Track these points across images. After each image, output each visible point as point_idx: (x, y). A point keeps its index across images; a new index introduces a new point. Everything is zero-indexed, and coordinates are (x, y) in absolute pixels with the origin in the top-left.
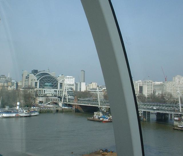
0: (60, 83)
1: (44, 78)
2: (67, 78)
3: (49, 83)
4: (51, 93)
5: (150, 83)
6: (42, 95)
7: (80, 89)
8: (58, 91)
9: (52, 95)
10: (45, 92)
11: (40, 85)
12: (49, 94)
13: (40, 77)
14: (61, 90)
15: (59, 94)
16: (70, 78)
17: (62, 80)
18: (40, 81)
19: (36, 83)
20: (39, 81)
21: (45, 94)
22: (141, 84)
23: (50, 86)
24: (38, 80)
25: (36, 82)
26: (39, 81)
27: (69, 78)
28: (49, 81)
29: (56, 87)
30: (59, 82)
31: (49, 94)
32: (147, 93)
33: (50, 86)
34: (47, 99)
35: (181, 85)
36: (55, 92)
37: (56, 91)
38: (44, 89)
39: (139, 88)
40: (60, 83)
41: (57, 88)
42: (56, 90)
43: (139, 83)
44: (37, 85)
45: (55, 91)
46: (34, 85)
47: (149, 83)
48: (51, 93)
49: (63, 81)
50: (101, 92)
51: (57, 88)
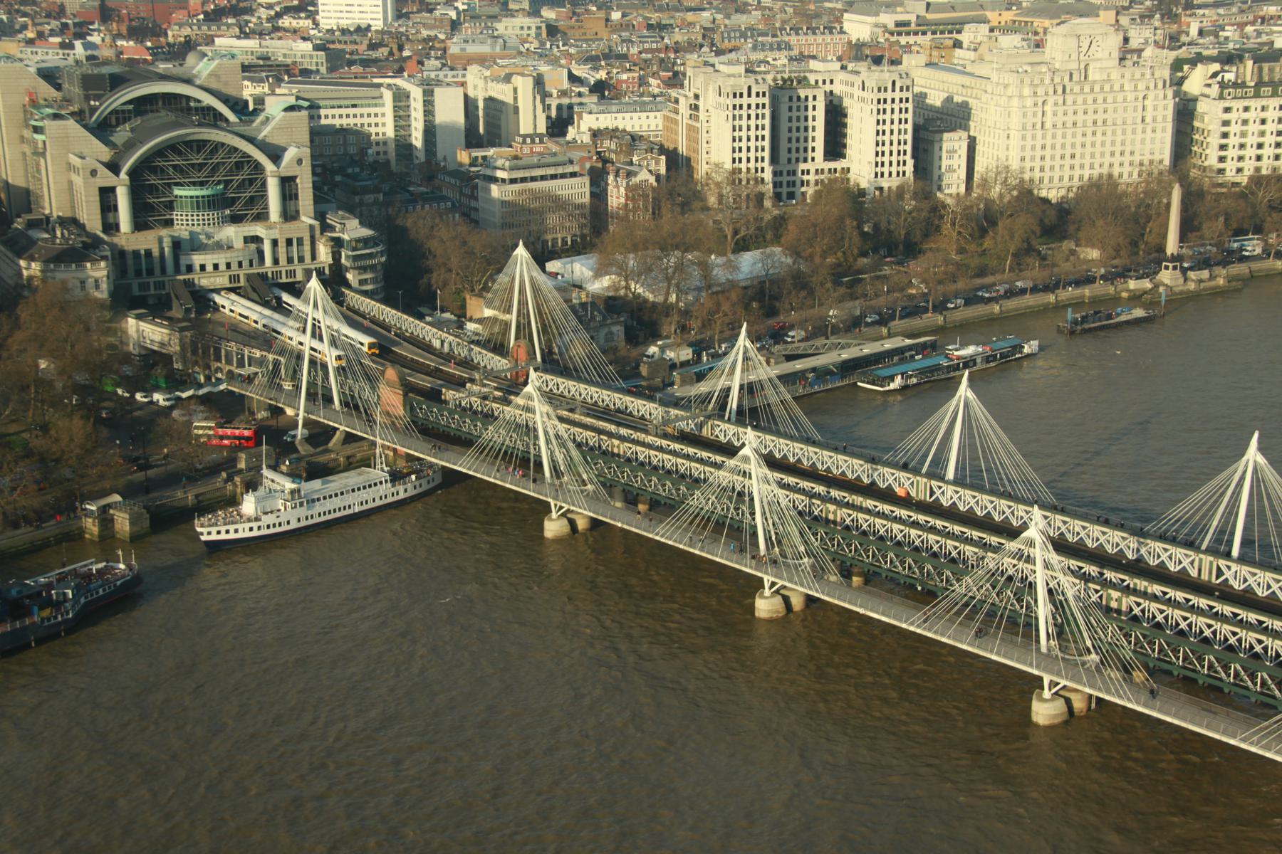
1: (159, 152)
3: (202, 184)
4: (222, 267)
6: (160, 285)
8: (275, 243)
9: (234, 279)
10: (184, 261)
12: (209, 268)
13: (130, 146)
14: (294, 230)
15: (283, 266)
18: (132, 173)
19: (107, 195)
20: (123, 175)
26: (123, 175)
28: (201, 166)
29: (253, 209)
31: (209, 268)
35: (1097, 89)
37: (257, 240)
41: (262, 217)
44: (116, 208)
46: (91, 218)
48: (222, 267)
49: (300, 162)
50: (573, 175)
51: (262, 217)
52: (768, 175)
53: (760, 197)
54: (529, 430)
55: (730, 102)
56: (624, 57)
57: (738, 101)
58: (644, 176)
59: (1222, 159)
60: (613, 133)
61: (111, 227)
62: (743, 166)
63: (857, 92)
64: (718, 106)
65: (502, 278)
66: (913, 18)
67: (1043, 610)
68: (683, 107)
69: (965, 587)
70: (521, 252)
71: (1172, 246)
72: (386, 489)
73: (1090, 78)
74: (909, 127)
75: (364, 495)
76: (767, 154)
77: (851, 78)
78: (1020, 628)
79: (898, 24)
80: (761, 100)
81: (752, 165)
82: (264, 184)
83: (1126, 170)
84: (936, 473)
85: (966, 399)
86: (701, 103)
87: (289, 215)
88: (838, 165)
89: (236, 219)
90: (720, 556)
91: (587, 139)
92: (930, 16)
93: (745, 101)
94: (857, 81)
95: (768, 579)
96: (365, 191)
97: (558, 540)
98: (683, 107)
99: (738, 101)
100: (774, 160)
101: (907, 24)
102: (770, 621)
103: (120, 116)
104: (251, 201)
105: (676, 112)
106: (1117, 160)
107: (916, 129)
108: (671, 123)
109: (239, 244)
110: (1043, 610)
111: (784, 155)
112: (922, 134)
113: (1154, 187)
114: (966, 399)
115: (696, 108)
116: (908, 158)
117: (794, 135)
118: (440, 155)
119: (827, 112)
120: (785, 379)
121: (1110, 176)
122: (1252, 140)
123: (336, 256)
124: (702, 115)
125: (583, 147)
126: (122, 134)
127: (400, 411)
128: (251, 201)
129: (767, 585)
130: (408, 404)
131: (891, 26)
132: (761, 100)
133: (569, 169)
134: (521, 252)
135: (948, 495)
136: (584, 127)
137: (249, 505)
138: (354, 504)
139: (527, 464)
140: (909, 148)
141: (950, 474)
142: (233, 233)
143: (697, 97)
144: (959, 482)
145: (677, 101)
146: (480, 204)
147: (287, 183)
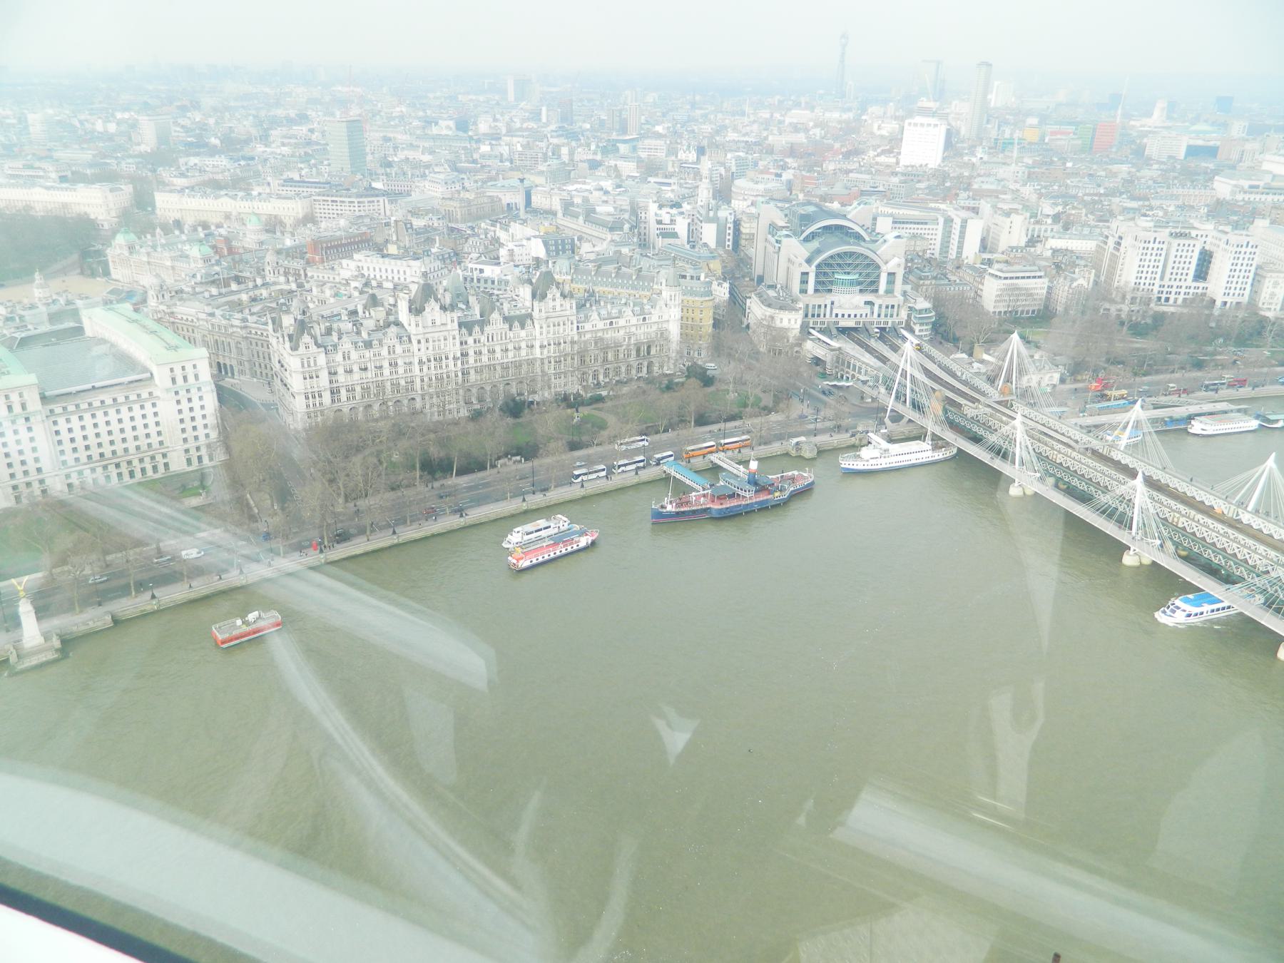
0: (889, 274)
2: (916, 125)
6: (823, 323)
7: (960, 247)
8: (880, 306)
10: (835, 312)
11: (818, 282)
13: (818, 252)
14: (890, 301)
16: (929, 125)
17: (895, 261)
18: (818, 266)
21: (834, 319)
22: (1209, 240)
23: (852, 283)
24: (809, 261)
25: (803, 274)
26: (813, 267)
27: (922, 125)
30: (884, 268)
32: (1224, 285)
33: (852, 283)
34: (838, 358)
36: (868, 310)
37: (870, 303)
38: (827, 299)
39: (1195, 261)
40: (889, 274)
42: (870, 297)
45: (867, 303)
51: (877, 291)
52: (1156, 289)
54: (1012, 441)
55: (1143, 245)
56: (1075, 197)
58: (1081, 281)
60: (1066, 252)
61: (804, 291)
63: (1223, 245)
65: (1004, 346)
66: (1261, 184)
68: (1111, 242)
70: (1015, 337)
72: (930, 453)
75: (919, 455)
76: (1158, 276)
77: (1220, 235)
79: (1251, 187)
82: (879, 276)
84: (1242, 504)
85: (1271, 470)
86: (1123, 242)
87: (889, 292)
88: (1201, 285)
89: (861, 291)
90: (1109, 528)
91: (1049, 253)
92: (1275, 184)
93: (1151, 245)
94: (1224, 238)
96: (926, 278)
97: (1016, 498)
98: (1111, 242)
100: (1162, 278)
101: (1257, 187)
102: (1130, 567)
103: (813, 236)
104: (873, 283)
105: (1106, 243)
107: (1258, 267)
108: (1100, 250)
109: (862, 304)
111: (1167, 276)
112: (1260, 271)
114: (1271, 470)
115: (1119, 244)
116: (1248, 287)
117: (1176, 265)
118: (964, 256)
119: (1201, 253)
120: (1154, 421)
123: (909, 316)
124: (1122, 249)
125: (1046, 259)
126: (815, 244)
127: (941, 413)
128: (873, 283)
130: (945, 411)
131: (1246, 187)
133: (1038, 274)
134: (1015, 337)
135: (1246, 518)
136: (1048, 246)
137: (865, 452)
138: (913, 459)
139: (1002, 454)
140: (1250, 281)
142: (860, 299)
143: (1121, 238)
144: (1257, 512)
145: (1107, 237)
146: (984, 288)
147: (891, 275)
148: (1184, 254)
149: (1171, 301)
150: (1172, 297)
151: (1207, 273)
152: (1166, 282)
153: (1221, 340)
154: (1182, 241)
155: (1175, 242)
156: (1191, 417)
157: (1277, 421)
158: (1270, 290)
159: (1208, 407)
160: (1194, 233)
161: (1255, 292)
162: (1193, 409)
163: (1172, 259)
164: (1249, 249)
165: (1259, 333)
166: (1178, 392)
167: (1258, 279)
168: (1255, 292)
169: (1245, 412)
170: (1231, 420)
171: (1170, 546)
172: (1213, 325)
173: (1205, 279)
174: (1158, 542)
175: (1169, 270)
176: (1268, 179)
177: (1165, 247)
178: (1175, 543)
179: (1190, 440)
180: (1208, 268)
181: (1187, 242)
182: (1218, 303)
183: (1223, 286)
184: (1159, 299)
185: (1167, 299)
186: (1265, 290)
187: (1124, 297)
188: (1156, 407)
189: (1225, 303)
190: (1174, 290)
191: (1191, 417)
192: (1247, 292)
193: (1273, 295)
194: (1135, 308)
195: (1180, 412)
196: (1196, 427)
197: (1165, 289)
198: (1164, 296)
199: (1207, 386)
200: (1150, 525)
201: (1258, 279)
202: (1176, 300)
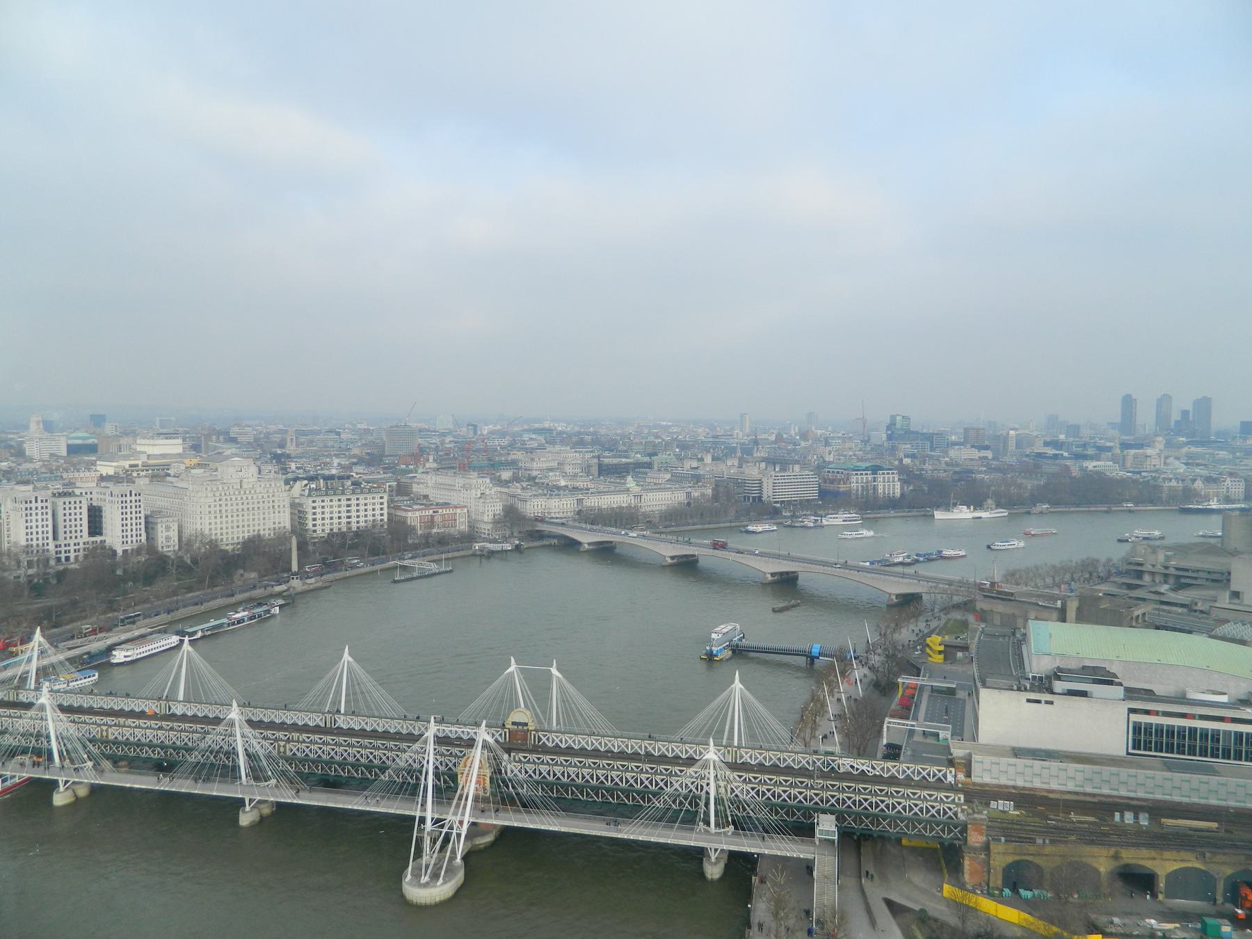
5: (133, 498)
22: (94, 496)
32: (120, 534)
43: (89, 496)
47: (128, 498)
52: (51, 547)
53: (48, 560)
55: (24, 506)
57: (28, 505)
59: (314, 525)
62: (34, 543)
63: (108, 498)
64: (15, 509)
66: (139, 463)
67: (242, 761)
69: (192, 758)
71: (295, 567)
73: (245, 486)
74: (142, 515)
76: (50, 535)
78: (230, 773)
79: (131, 466)
80: (44, 504)
81: (40, 542)
83: (267, 532)
88: (98, 539)
92: (151, 462)
95: (61, 780)
99: (28, 505)
100: (55, 538)
101: (137, 466)
106: (262, 527)
107: (146, 517)
110: (242, 761)
111: (61, 535)
112: (151, 520)
113: (281, 538)
117: (68, 523)
121: (259, 535)
122: (327, 516)
129: (61, 784)
132: (44, 504)
140: (143, 527)
141: (181, 697)
144: (187, 700)
148: (73, 511)
149: (72, 559)
150: (72, 555)
151: (101, 528)
152: (61, 541)
153: (130, 583)
154: (67, 500)
155: (60, 501)
156: (110, 649)
157: (195, 632)
158: (165, 534)
159: (123, 637)
160: (77, 492)
161: (150, 538)
162: (109, 642)
163: (60, 518)
164: (133, 498)
165: (164, 569)
166: (94, 632)
167: (149, 525)
168: (150, 538)
169: (165, 631)
170: (152, 641)
171: (107, 765)
172: (119, 572)
173: (101, 534)
174: (90, 764)
175: (61, 530)
176: (144, 458)
177: (49, 504)
178: (108, 758)
179: (116, 670)
180: (101, 523)
181: (72, 500)
182: (120, 552)
183: (119, 535)
184: (59, 559)
185: (67, 559)
186: (160, 534)
187: (19, 563)
188: (69, 649)
189: (125, 551)
190: (72, 548)
191: (110, 649)
192: (144, 538)
193: (168, 538)
194: (30, 572)
195: (96, 645)
196: (119, 656)
197: (63, 549)
198: (63, 556)
199: (122, 621)
200: (76, 751)
201: (149, 525)
202: (76, 557)
